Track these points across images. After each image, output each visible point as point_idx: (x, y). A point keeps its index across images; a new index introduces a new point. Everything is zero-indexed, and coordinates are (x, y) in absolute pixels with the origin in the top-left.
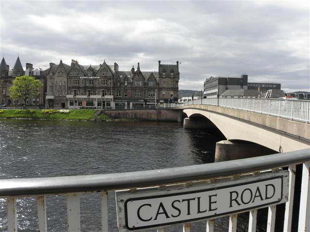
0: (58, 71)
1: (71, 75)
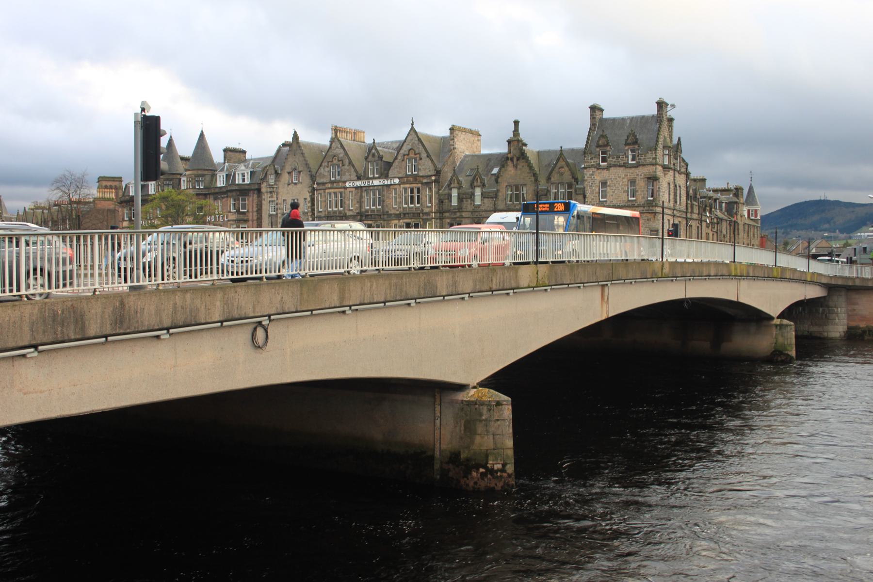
0: (288, 168)
1: (324, 176)
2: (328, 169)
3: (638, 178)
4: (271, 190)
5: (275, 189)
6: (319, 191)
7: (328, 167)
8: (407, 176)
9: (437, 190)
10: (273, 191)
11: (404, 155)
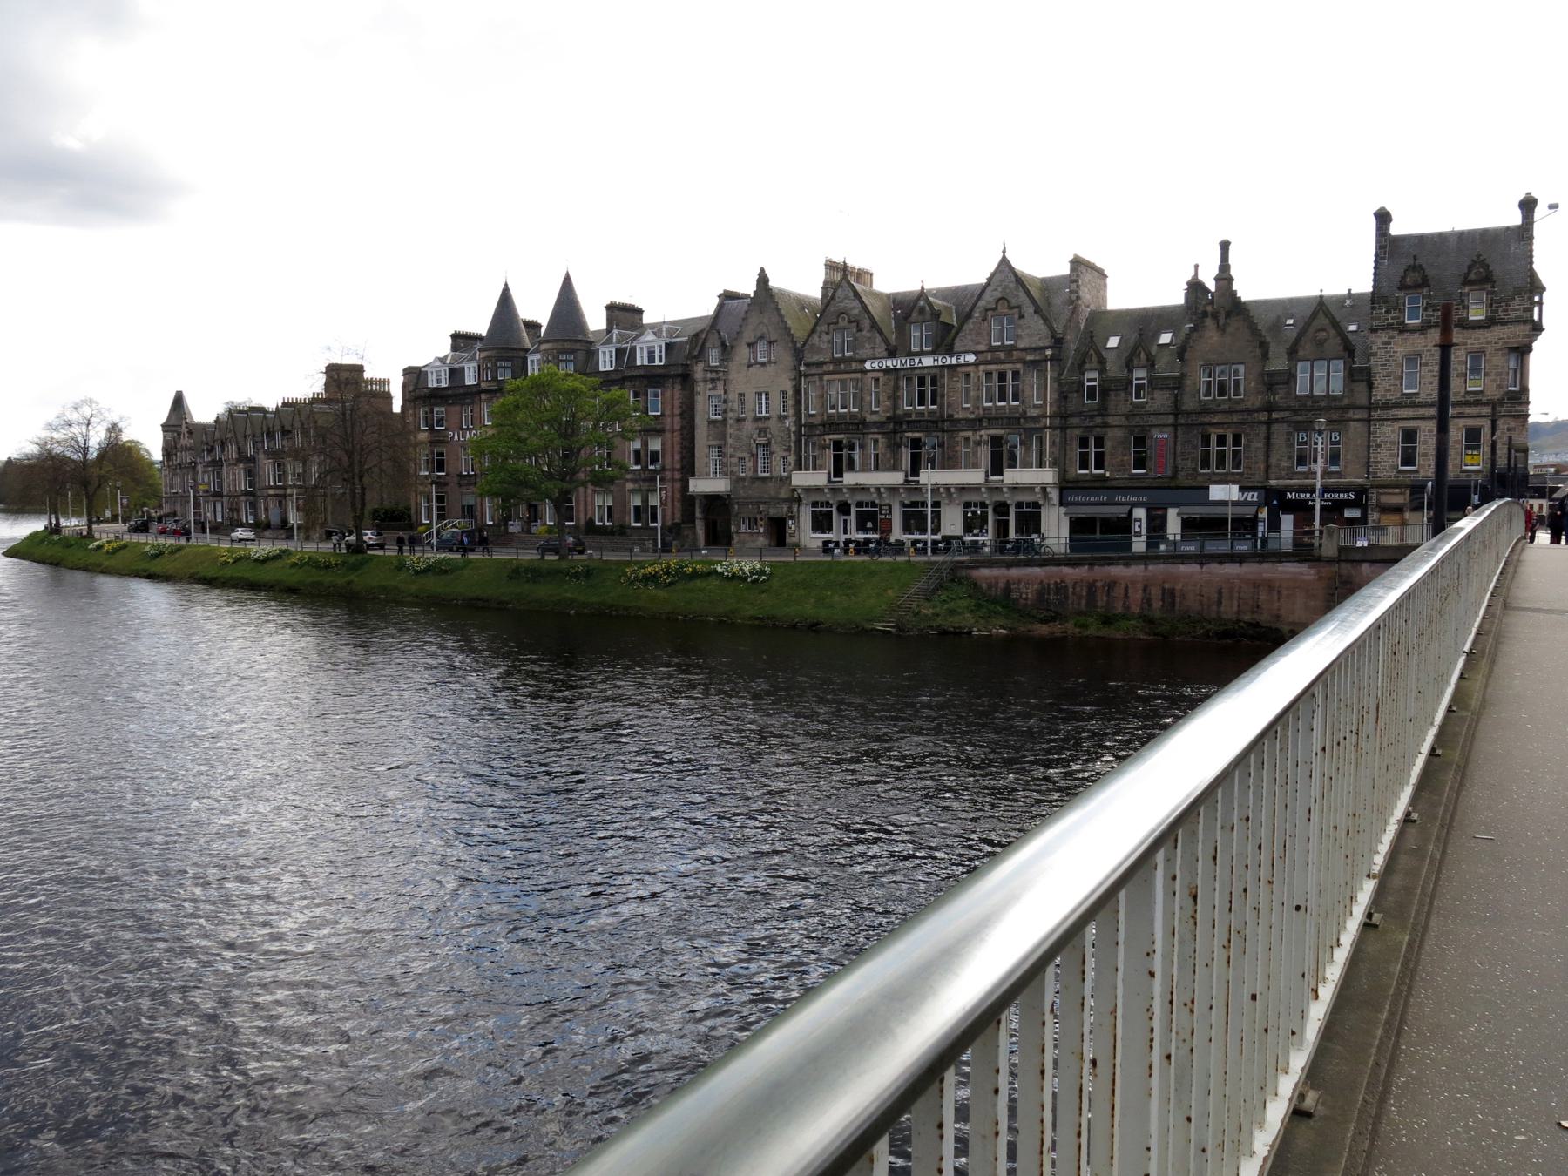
0: (749, 336)
1: (819, 351)
2: (829, 337)
5: (721, 374)
6: (810, 379)
7: (827, 333)
8: (992, 349)
9: (1055, 375)
10: (717, 377)
11: (987, 310)
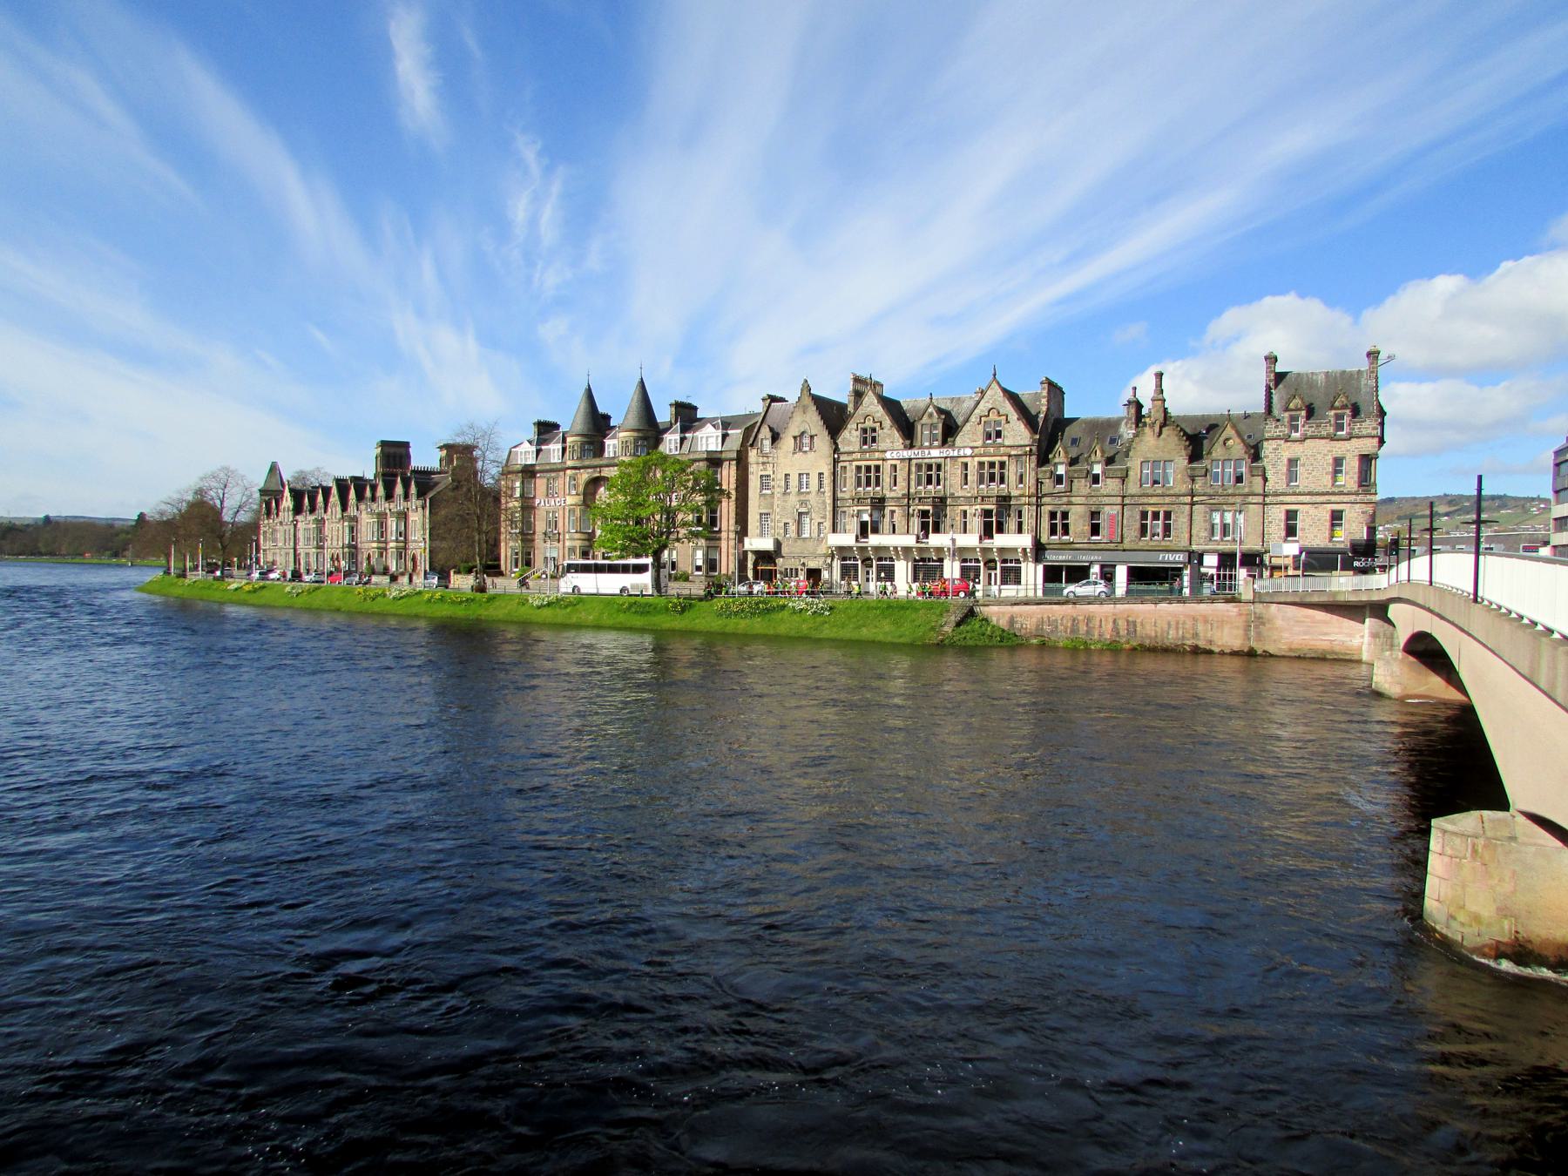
0: (794, 430)
1: (850, 443)
3: (1348, 456)
4: (765, 459)
9: (1033, 465)
